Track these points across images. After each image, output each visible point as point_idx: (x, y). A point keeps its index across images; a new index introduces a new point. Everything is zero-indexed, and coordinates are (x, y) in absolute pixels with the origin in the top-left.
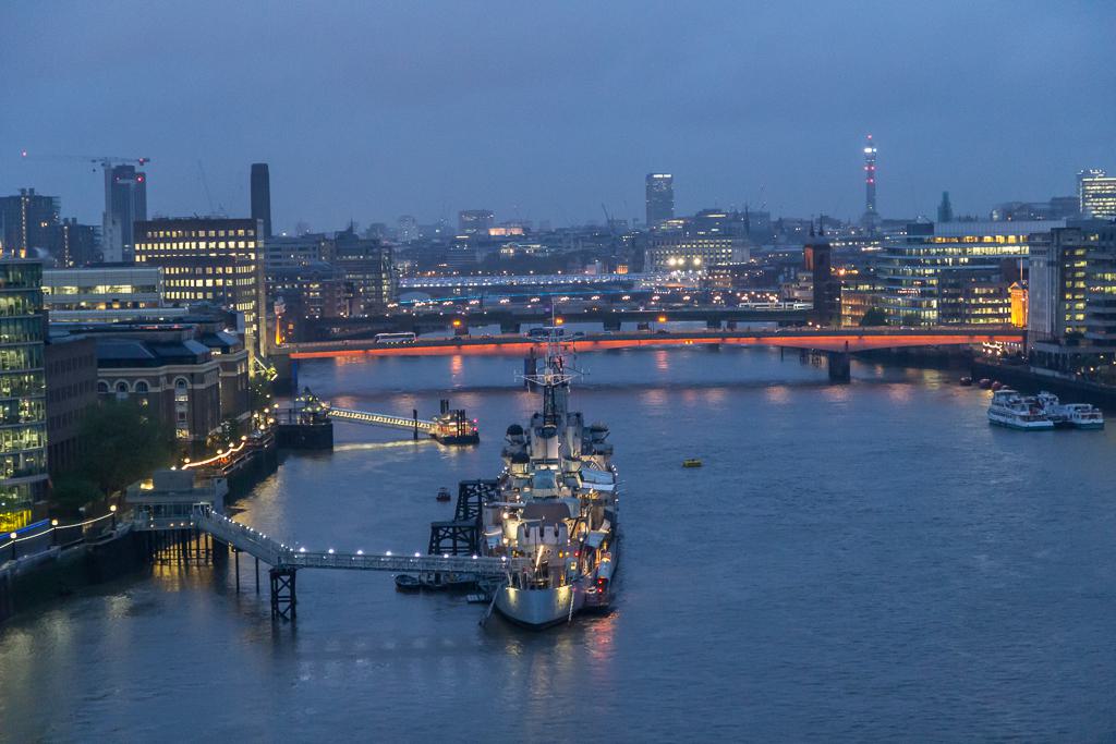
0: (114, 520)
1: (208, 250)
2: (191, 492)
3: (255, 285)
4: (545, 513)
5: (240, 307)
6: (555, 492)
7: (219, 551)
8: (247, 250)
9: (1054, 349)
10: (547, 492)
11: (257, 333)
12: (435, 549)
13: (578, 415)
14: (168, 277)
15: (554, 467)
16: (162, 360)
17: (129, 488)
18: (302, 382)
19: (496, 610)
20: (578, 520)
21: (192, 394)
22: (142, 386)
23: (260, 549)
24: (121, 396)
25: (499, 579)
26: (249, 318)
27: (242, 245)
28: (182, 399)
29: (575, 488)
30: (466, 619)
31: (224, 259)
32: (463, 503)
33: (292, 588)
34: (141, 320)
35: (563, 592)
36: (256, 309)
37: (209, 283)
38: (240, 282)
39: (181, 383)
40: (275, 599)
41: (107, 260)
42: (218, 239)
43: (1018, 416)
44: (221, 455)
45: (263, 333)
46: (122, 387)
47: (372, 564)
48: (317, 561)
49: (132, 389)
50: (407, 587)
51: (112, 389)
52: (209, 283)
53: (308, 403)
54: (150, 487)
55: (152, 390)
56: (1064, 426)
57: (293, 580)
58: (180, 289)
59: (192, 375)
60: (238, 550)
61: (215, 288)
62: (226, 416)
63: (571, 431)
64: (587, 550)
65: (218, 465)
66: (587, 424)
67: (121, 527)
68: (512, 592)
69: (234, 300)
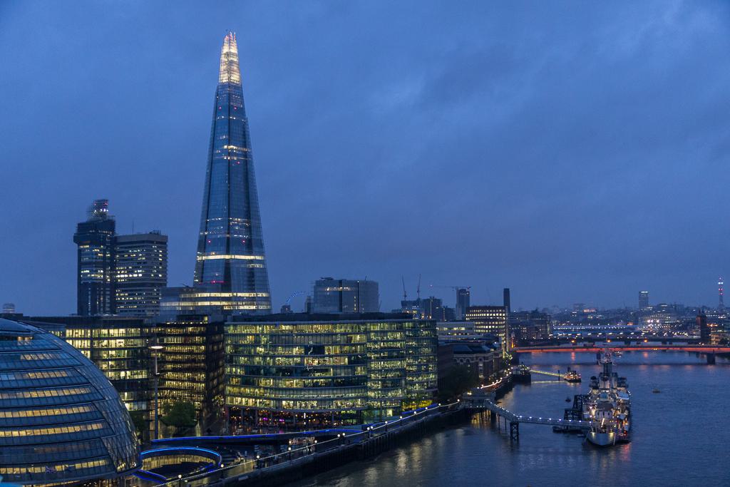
0: (459, 404)
1: (489, 316)
2: (485, 396)
4: (605, 407)
5: (500, 335)
6: (608, 400)
7: (493, 416)
8: (502, 316)
10: (605, 400)
11: (505, 344)
12: (566, 418)
13: (616, 373)
14: (477, 325)
16: (474, 352)
17: (464, 394)
18: (521, 360)
19: (588, 439)
20: (617, 410)
21: (484, 363)
22: (468, 360)
23: (507, 416)
25: (589, 429)
26: (503, 339)
27: (501, 315)
28: (481, 365)
29: (615, 398)
30: (577, 443)
31: (495, 320)
32: (576, 402)
33: (517, 429)
34: (468, 339)
36: (505, 336)
37: (490, 327)
38: (500, 327)
39: (481, 360)
40: (512, 432)
42: (493, 313)
44: (494, 384)
45: (508, 344)
46: (462, 361)
47: (544, 422)
48: (525, 421)
50: (556, 431)
51: (458, 361)
52: (490, 327)
53: (523, 367)
55: (471, 362)
57: (518, 426)
58: (481, 329)
59: (484, 357)
61: (492, 329)
63: (613, 379)
64: (620, 420)
65: (492, 387)
66: (619, 377)
68: (593, 434)
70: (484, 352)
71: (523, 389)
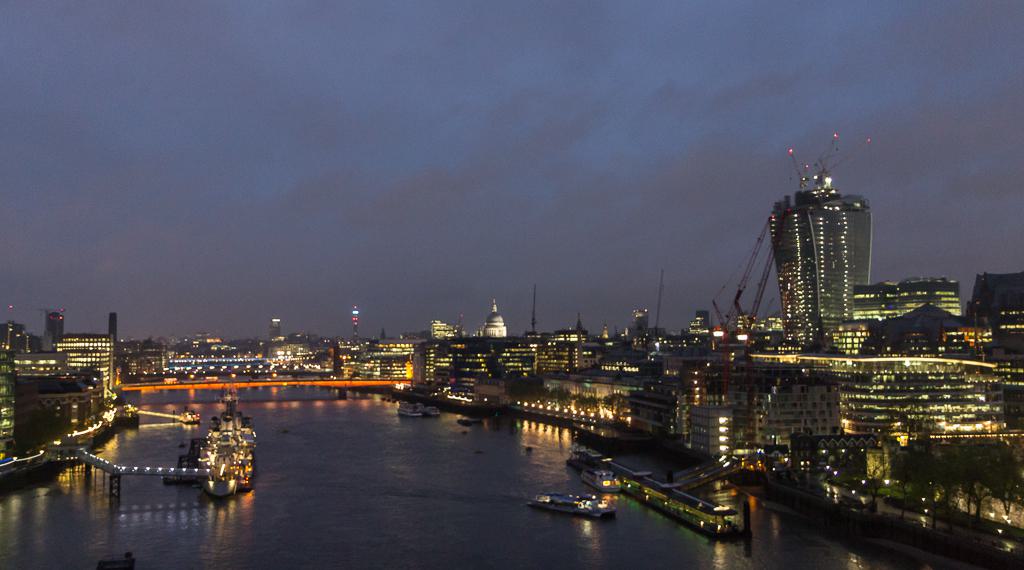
2: (78, 445)
3: (109, 361)
4: (226, 452)
5: (102, 369)
7: (88, 468)
9: (422, 387)
15: (230, 433)
18: (127, 398)
19: (205, 491)
21: (79, 405)
24: (48, 405)
25: (206, 478)
29: (237, 441)
31: (96, 351)
32: (192, 448)
34: (58, 375)
35: (232, 483)
36: (109, 370)
37: (89, 360)
39: (75, 401)
40: (111, 488)
41: (44, 349)
43: (409, 412)
44: (90, 429)
47: (153, 474)
48: (129, 472)
49: (53, 403)
51: (44, 403)
54: (58, 443)
56: (426, 415)
60: (96, 468)
61: (91, 362)
62: (94, 413)
64: (243, 466)
65: (89, 433)
66: (245, 415)
67: (44, 460)
68: (211, 483)
69: (99, 367)
70: (80, 390)
71: (130, 435)
